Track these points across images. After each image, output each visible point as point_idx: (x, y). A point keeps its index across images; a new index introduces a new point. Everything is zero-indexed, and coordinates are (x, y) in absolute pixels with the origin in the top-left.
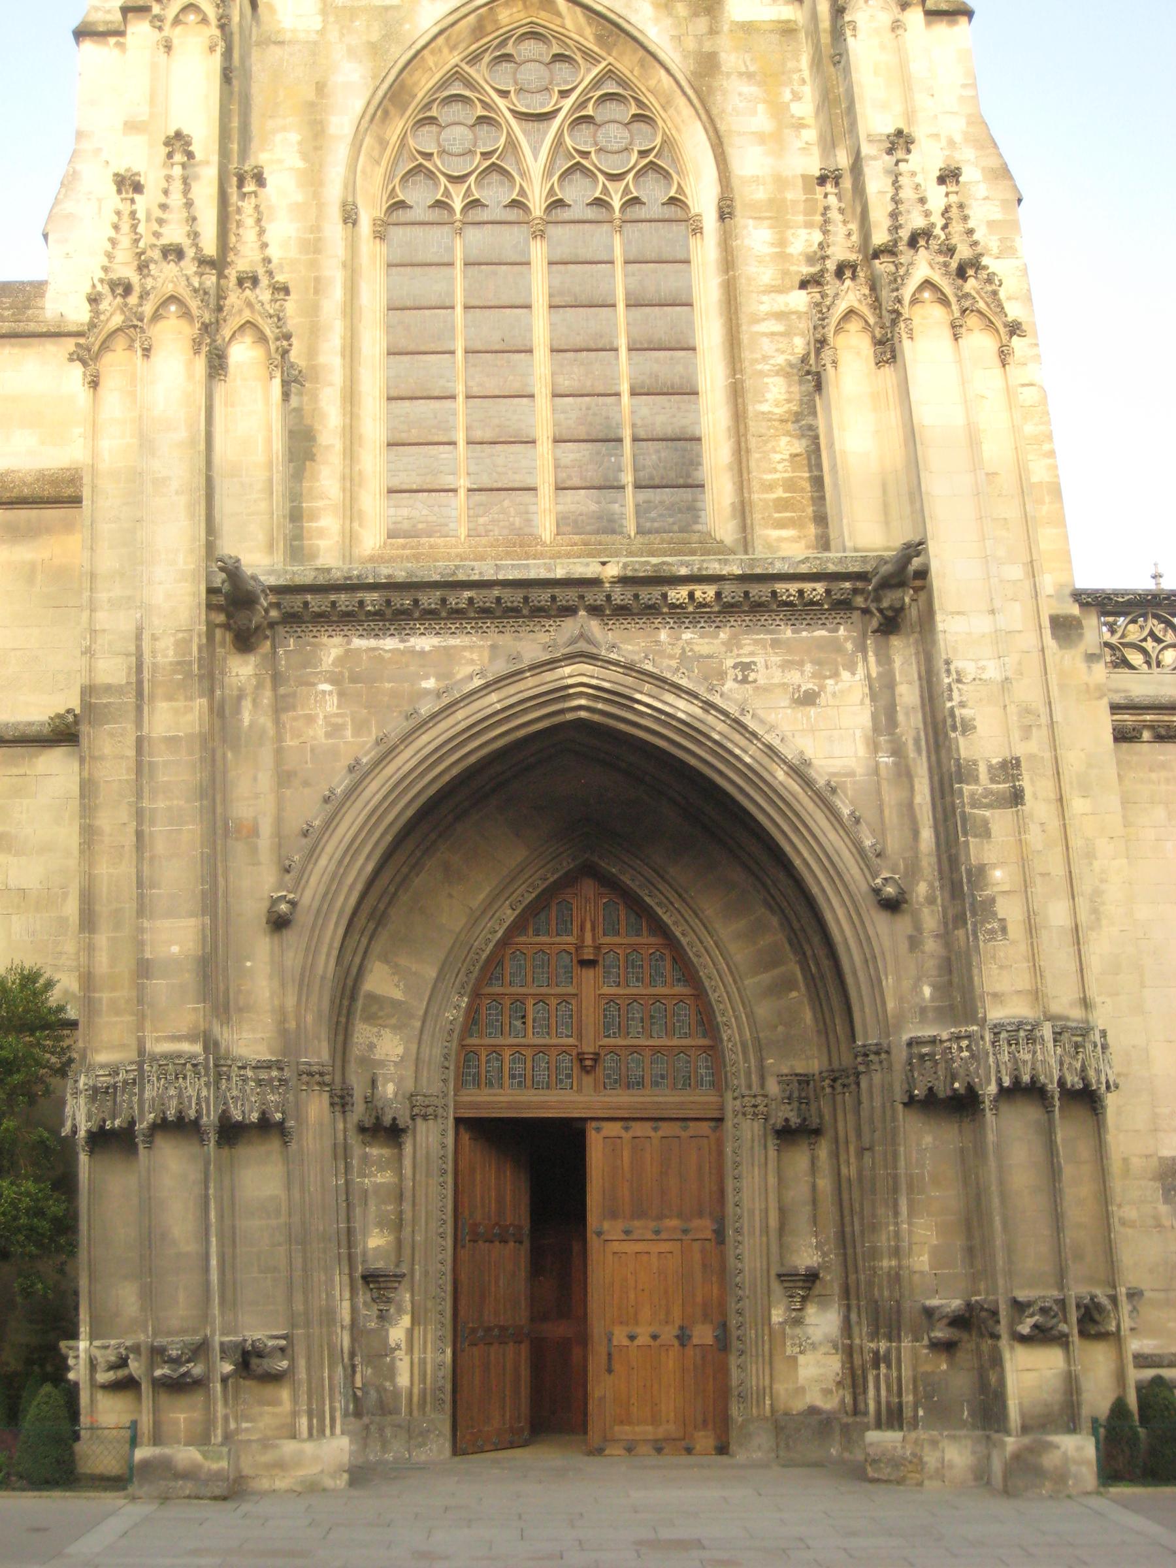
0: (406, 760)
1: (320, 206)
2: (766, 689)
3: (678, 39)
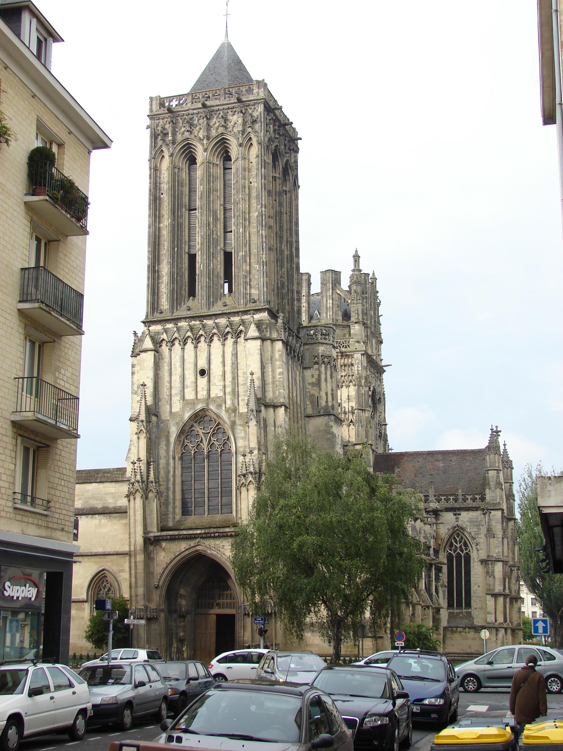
0: (174, 562)
1: (169, 456)
2: (226, 549)
3: (229, 418)
